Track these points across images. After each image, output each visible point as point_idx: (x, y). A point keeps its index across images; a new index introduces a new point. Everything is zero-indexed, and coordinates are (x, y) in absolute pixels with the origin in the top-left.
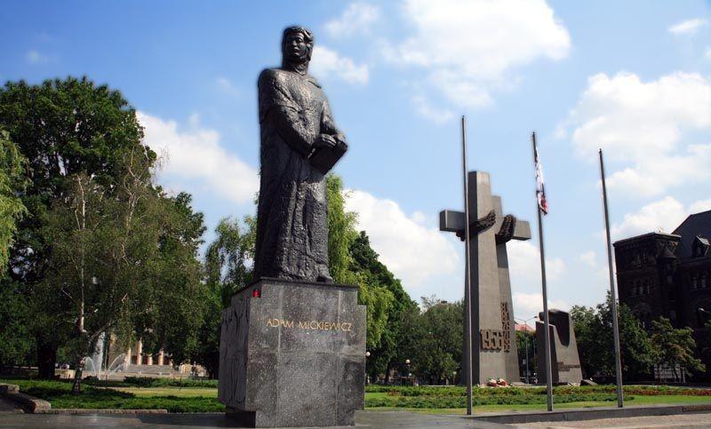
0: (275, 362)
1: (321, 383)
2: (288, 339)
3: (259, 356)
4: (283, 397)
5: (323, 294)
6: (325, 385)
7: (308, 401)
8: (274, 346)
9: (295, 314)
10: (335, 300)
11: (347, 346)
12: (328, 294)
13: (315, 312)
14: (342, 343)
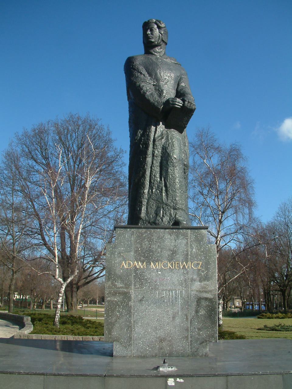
0: (129, 299)
1: (174, 318)
2: (140, 277)
3: (115, 294)
4: (138, 330)
5: (173, 237)
6: (178, 320)
7: (161, 333)
8: (128, 286)
9: (147, 256)
10: (184, 241)
11: (199, 283)
12: (177, 236)
13: (166, 253)
14: (193, 280)
